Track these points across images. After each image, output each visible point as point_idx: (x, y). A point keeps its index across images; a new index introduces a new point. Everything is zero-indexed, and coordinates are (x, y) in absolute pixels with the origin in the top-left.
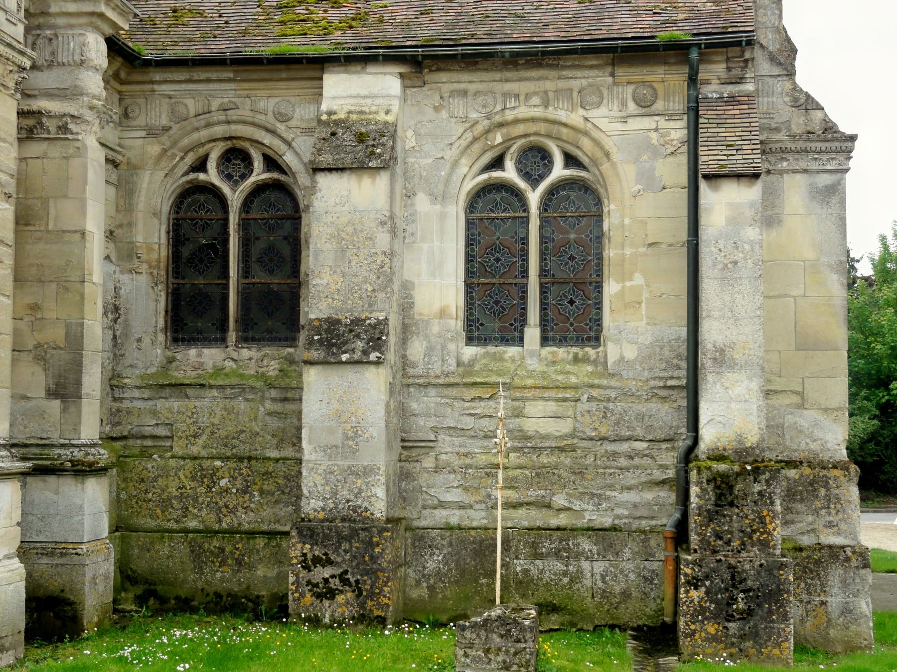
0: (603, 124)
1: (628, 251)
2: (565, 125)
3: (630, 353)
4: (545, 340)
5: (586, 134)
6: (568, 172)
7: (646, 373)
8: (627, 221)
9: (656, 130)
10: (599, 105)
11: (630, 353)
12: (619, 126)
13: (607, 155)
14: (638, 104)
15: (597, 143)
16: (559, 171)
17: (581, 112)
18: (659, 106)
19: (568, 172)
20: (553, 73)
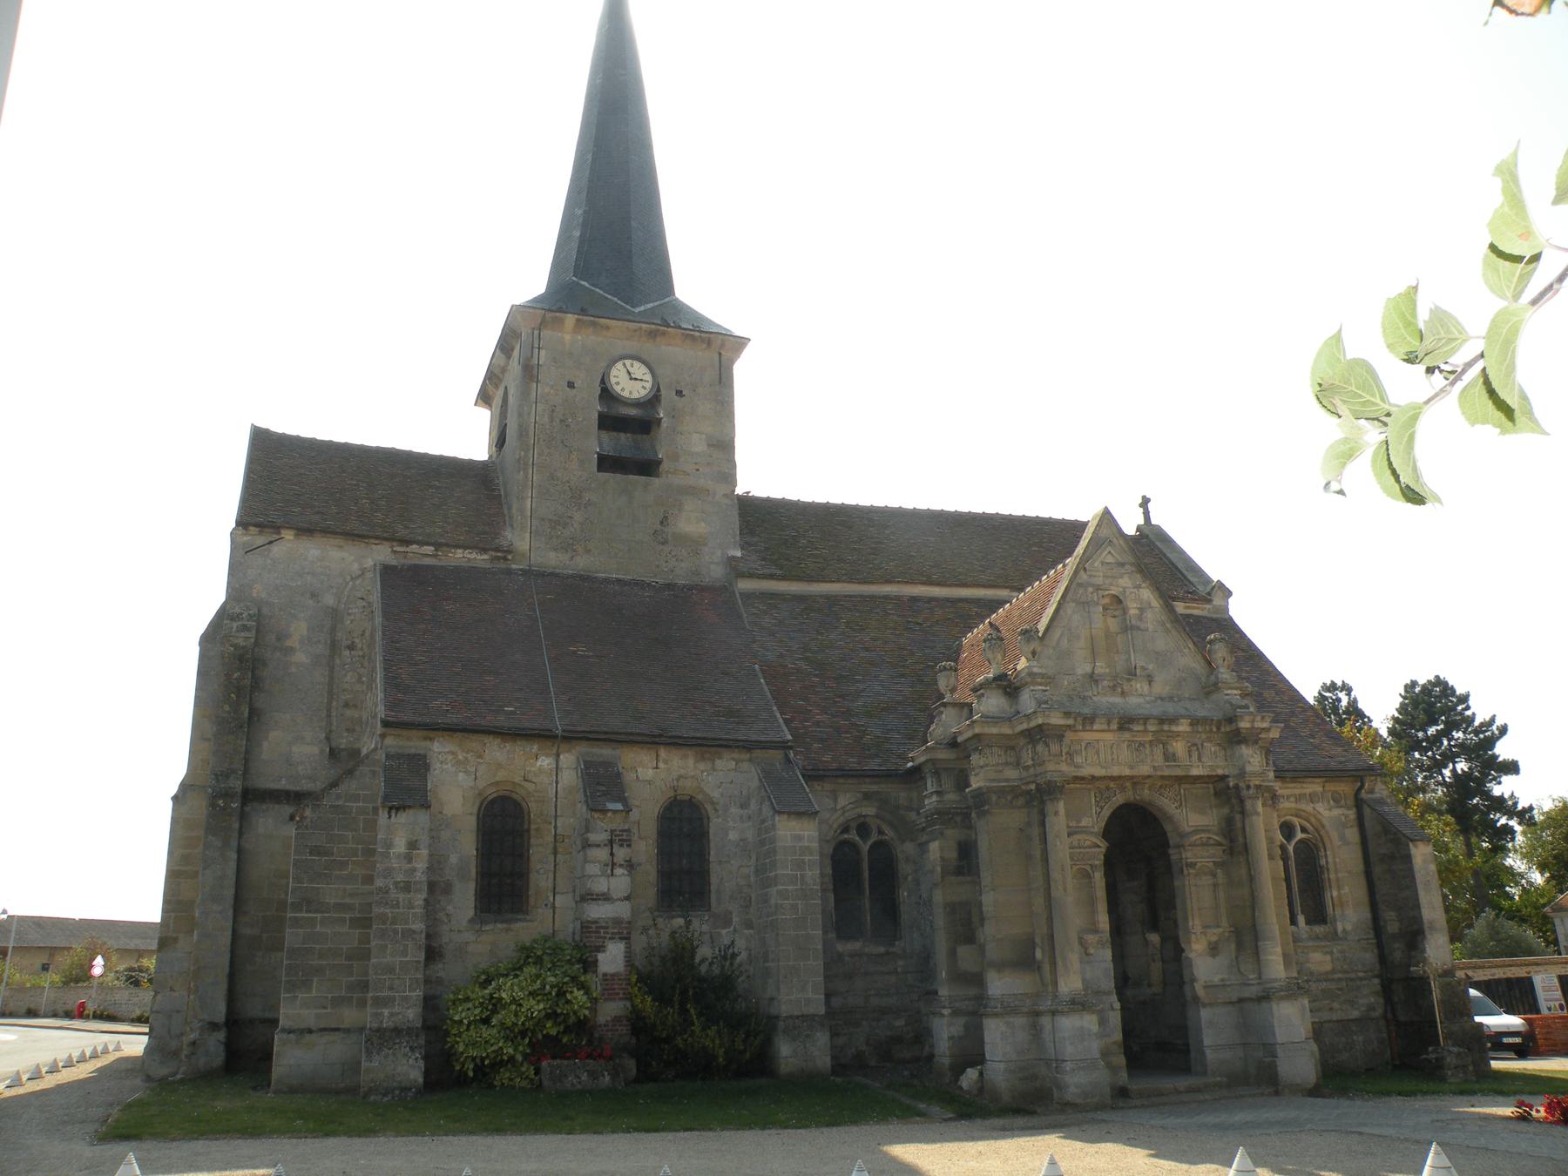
0: (1321, 810)
1: (1340, 875)
2: (1304, 811)
3: (1349, 927)
4: (1308, 922)
5: (1315, 816)
6: (1304, 836)
7: (1357, 938)
8: (1337, 860)
9: (1343, 814)
10: (1318, 802)
11: (1349, 927)
12: (1327, 812)
13: (1323, 826)
14: (1334, 800)
15: (1319, 820)
16: (1300, 835)
17: (1312, 805)
18: (1343, 802)
19: (1304, 836)
20: (1299, 785)
